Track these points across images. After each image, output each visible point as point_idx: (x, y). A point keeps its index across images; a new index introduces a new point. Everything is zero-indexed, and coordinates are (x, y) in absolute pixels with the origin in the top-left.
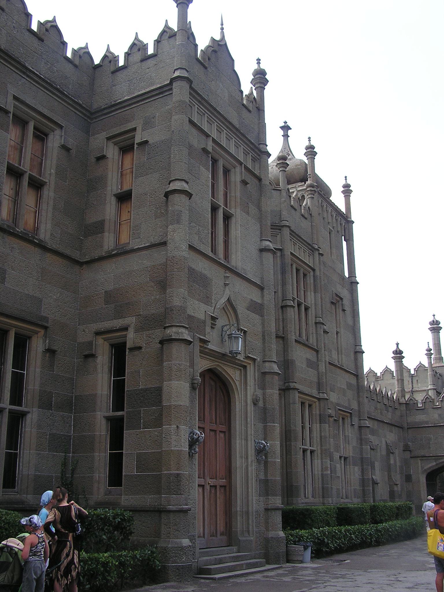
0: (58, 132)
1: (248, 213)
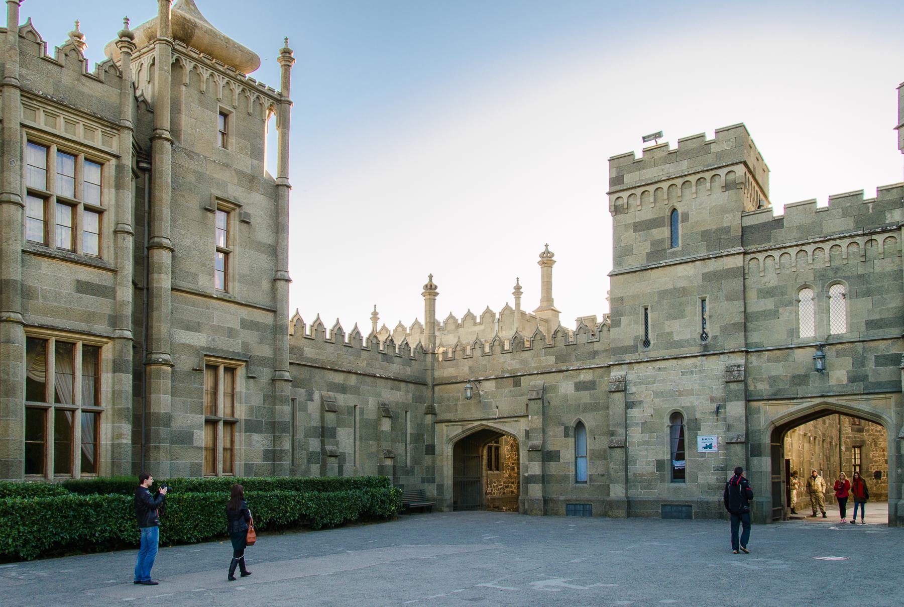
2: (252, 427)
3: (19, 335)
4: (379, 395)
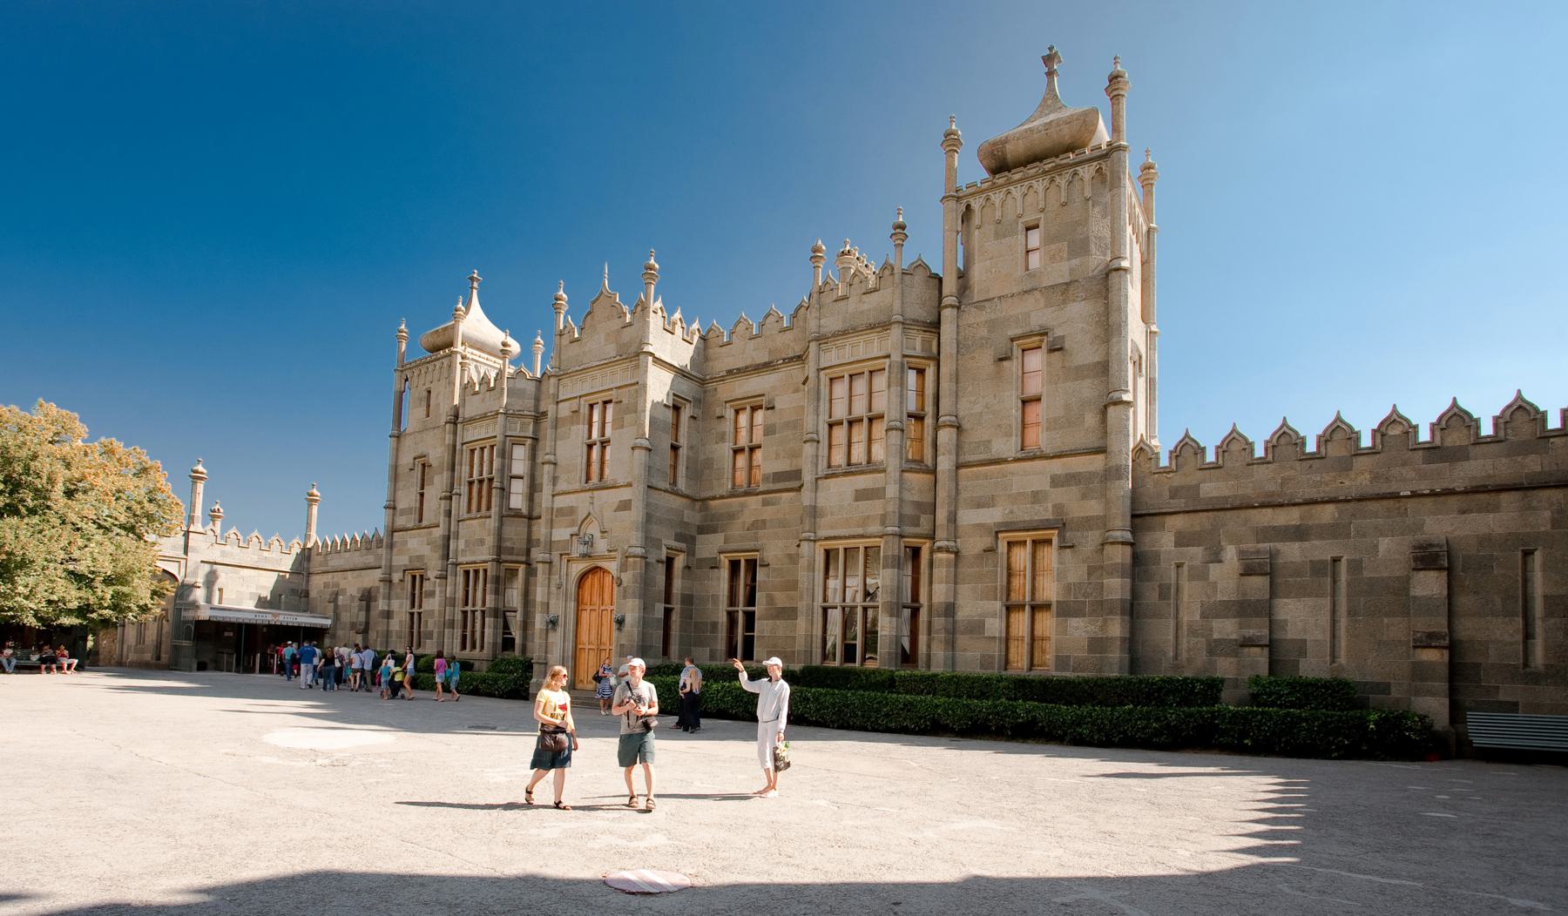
2: (1066, 610)
4: (1419, 527)
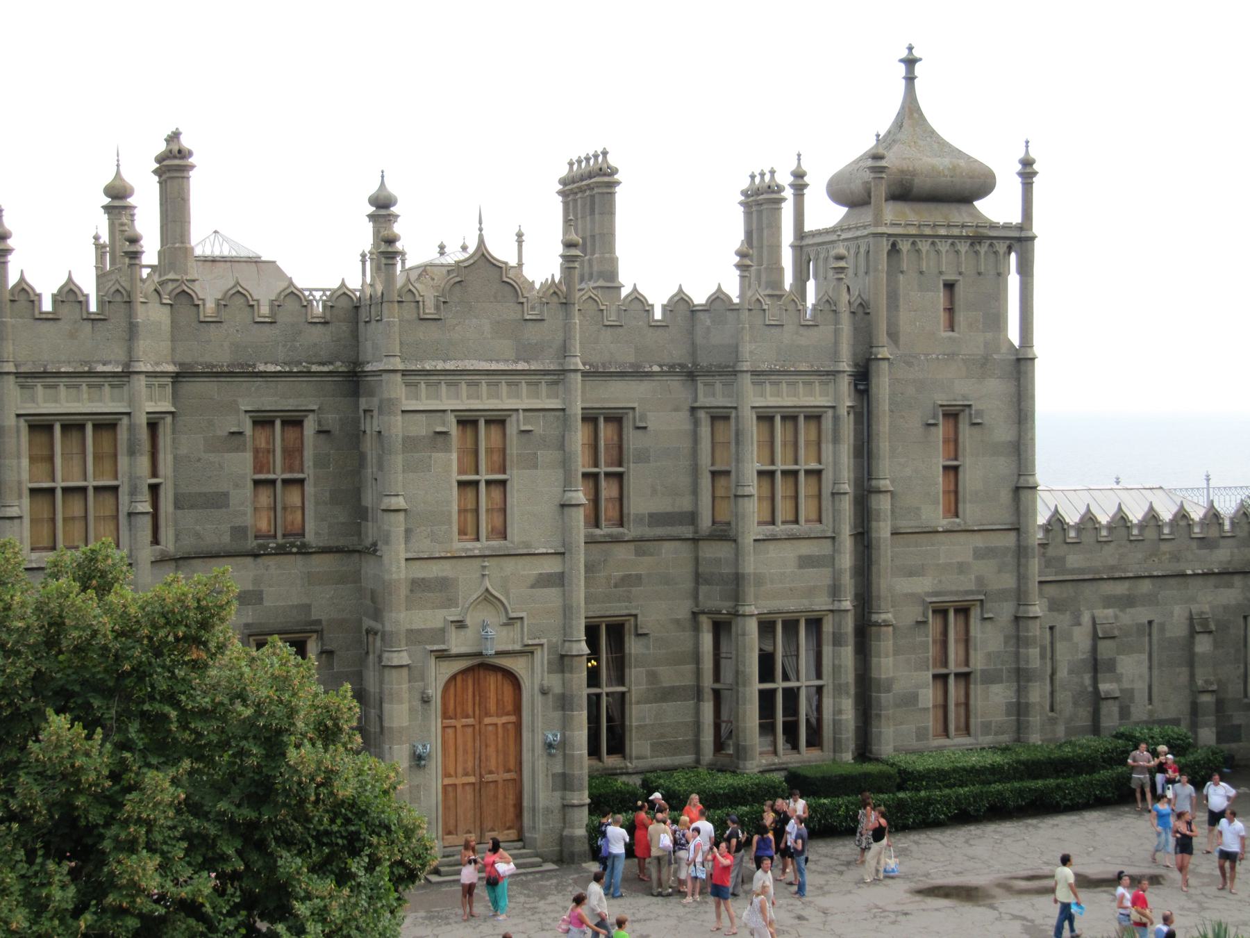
0: (311, 416)
1: (535, 467)
2: (990, 678)
3: (752, 626)
